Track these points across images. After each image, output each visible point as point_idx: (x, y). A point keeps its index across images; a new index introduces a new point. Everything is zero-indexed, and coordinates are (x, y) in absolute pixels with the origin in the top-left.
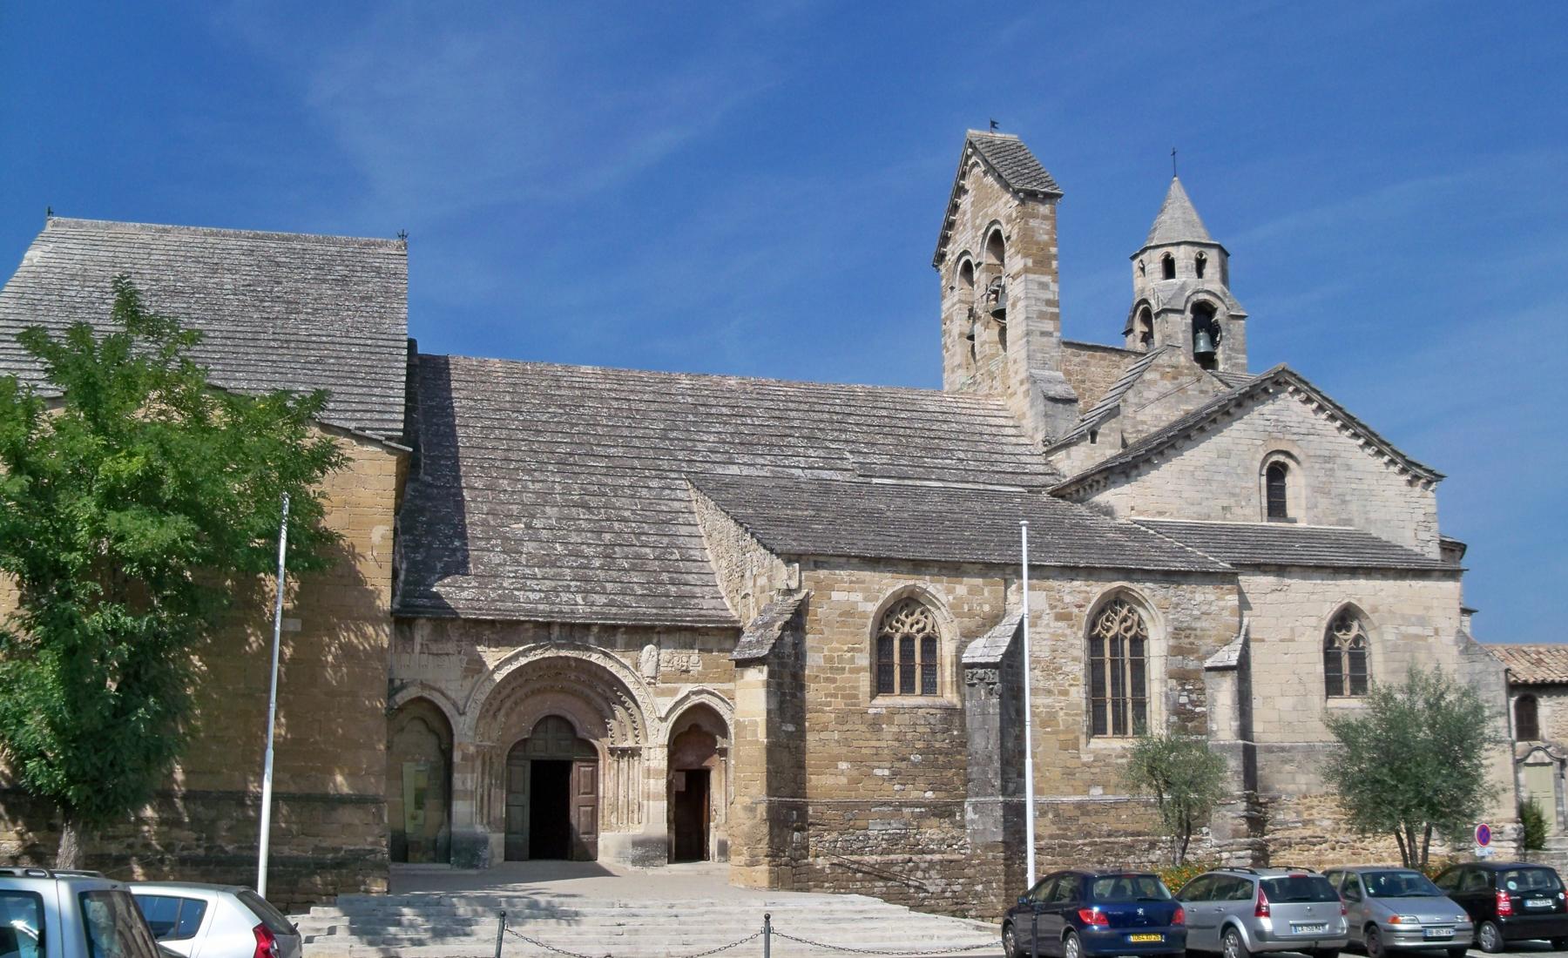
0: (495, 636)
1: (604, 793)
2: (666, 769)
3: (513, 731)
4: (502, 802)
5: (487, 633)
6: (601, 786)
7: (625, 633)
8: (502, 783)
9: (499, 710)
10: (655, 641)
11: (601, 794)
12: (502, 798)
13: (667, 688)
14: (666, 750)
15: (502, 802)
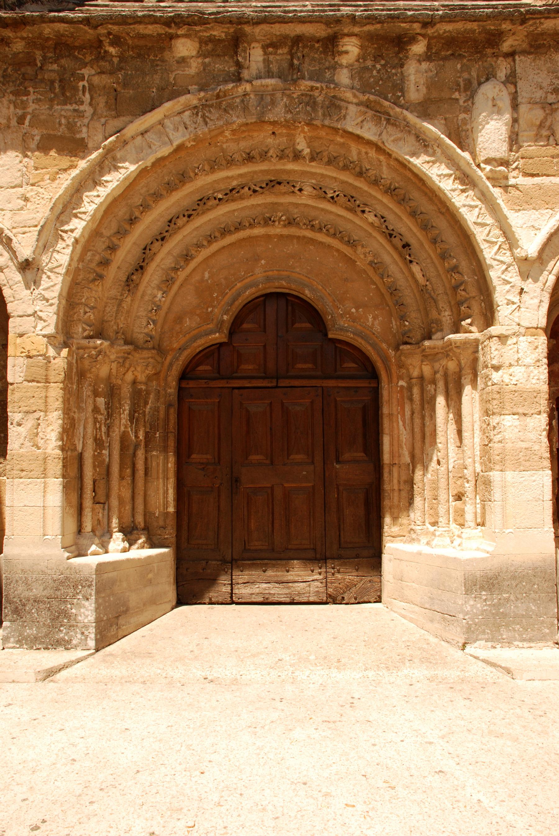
0: (106, 80)
1: (392, 452)
2: (545, 388)
3: (187, 322)
4: (165, 485)
5: (86, 72)
6: (386, 441)
7: (428, 57)
8: (165, 439)
9: (140, 268)
10: (502, 74)
11: (386, 458)
12: (166, 470)
13: (540, 187)
14: (542, 341)
15: (165, 485)
